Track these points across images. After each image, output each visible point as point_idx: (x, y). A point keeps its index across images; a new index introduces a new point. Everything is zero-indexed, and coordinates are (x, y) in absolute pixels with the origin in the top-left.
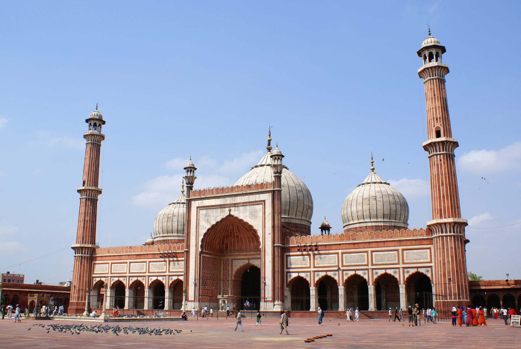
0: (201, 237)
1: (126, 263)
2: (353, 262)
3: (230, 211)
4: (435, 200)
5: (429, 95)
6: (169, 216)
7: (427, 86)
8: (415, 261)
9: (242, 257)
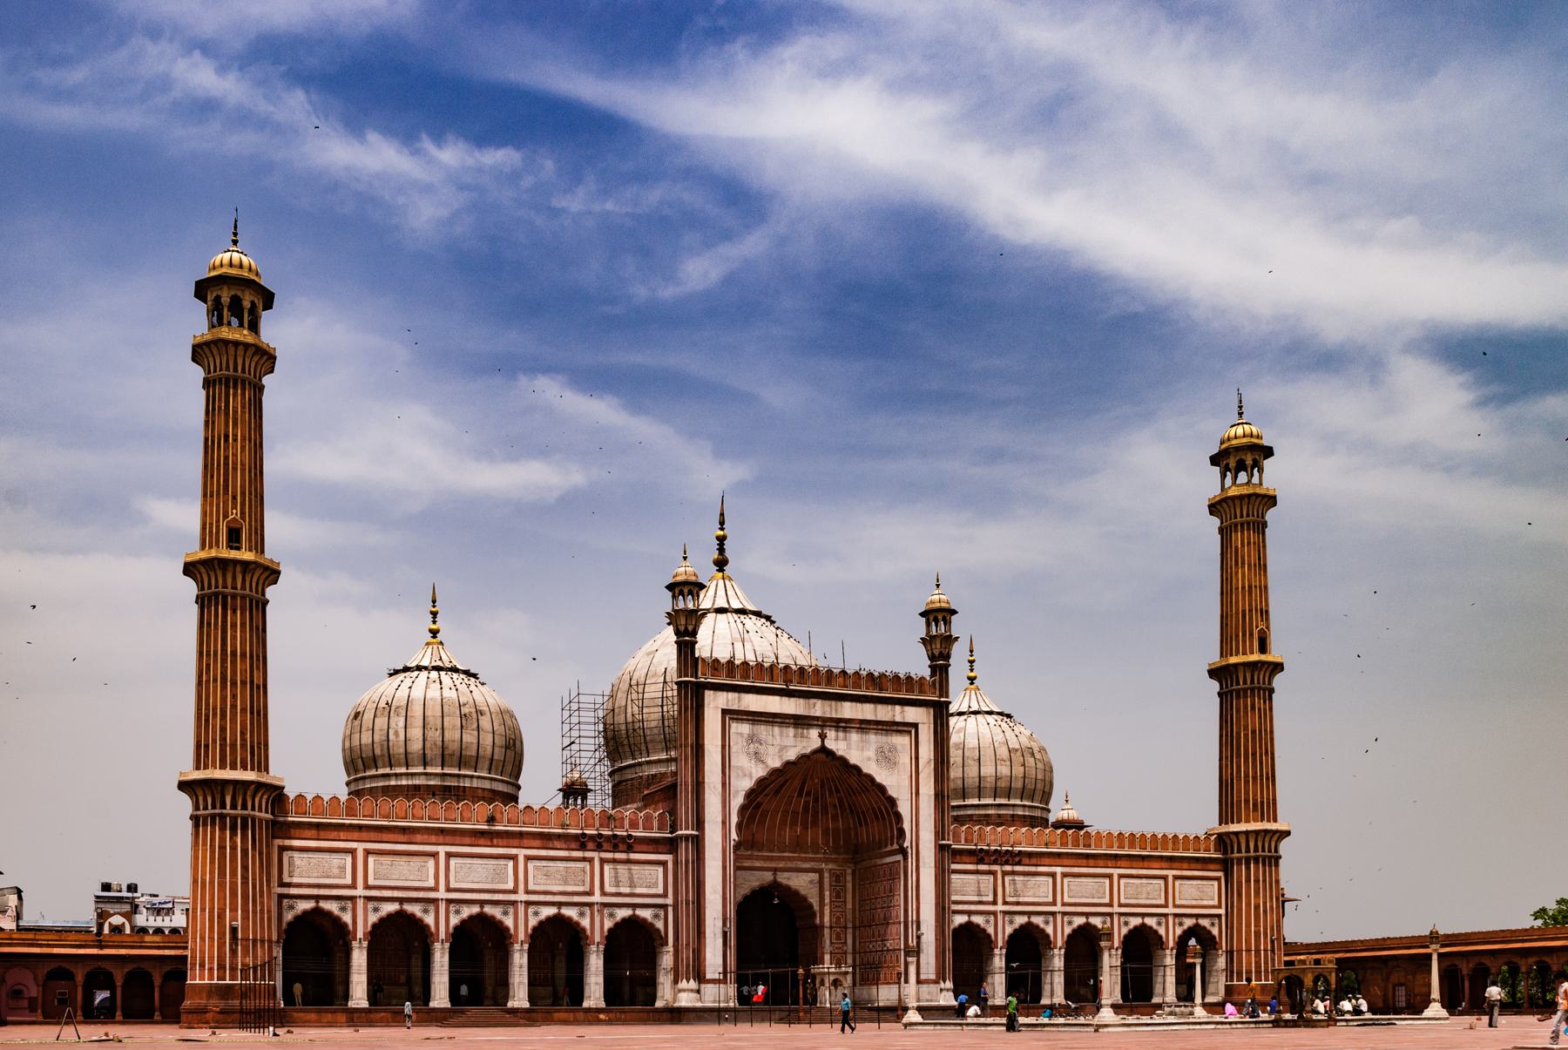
0: (737, 801)
1: (435, 855)
2: (1082, 897)
3: (823, 737)
6: (465, 710)
9: (758, 864)
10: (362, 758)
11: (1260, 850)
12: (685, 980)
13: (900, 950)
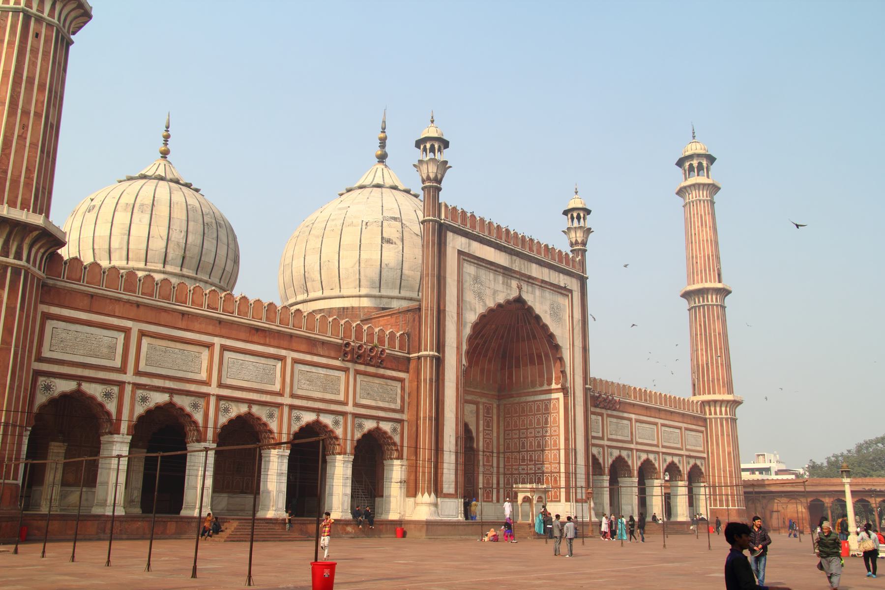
0: (467, 331)
1: (209, 346)
3: (520, 288)
4: (717, 367)
5: (709, 222)
7: (704, 207)
8: (693, 448)
10: (94, 250)
12: (426, 493)
13: (559, 472)
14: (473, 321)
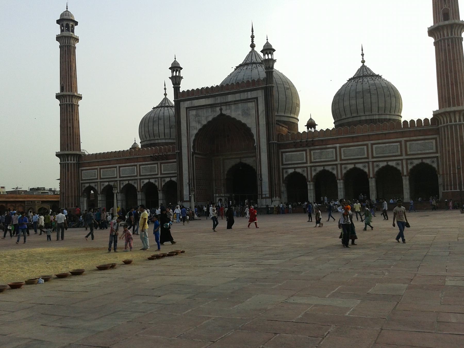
0: (193, 138)
1: (116, 167)
3: (221, 110)
8: (419, 152)
11: (449, 122)
14: (196, 133)
